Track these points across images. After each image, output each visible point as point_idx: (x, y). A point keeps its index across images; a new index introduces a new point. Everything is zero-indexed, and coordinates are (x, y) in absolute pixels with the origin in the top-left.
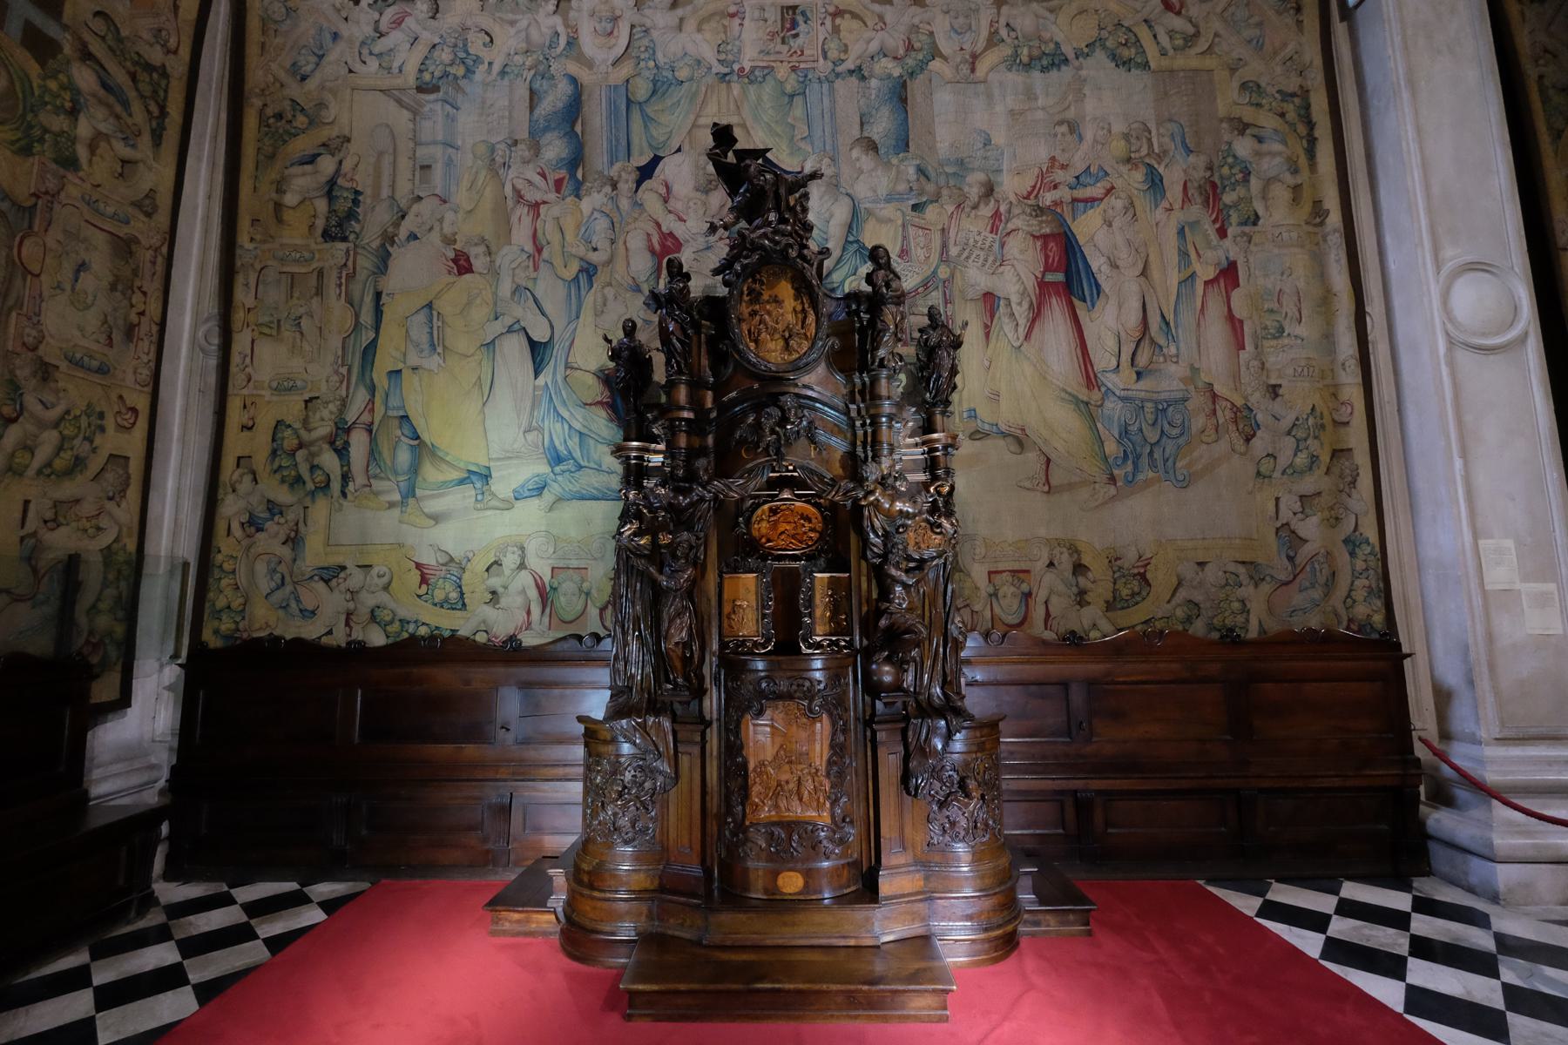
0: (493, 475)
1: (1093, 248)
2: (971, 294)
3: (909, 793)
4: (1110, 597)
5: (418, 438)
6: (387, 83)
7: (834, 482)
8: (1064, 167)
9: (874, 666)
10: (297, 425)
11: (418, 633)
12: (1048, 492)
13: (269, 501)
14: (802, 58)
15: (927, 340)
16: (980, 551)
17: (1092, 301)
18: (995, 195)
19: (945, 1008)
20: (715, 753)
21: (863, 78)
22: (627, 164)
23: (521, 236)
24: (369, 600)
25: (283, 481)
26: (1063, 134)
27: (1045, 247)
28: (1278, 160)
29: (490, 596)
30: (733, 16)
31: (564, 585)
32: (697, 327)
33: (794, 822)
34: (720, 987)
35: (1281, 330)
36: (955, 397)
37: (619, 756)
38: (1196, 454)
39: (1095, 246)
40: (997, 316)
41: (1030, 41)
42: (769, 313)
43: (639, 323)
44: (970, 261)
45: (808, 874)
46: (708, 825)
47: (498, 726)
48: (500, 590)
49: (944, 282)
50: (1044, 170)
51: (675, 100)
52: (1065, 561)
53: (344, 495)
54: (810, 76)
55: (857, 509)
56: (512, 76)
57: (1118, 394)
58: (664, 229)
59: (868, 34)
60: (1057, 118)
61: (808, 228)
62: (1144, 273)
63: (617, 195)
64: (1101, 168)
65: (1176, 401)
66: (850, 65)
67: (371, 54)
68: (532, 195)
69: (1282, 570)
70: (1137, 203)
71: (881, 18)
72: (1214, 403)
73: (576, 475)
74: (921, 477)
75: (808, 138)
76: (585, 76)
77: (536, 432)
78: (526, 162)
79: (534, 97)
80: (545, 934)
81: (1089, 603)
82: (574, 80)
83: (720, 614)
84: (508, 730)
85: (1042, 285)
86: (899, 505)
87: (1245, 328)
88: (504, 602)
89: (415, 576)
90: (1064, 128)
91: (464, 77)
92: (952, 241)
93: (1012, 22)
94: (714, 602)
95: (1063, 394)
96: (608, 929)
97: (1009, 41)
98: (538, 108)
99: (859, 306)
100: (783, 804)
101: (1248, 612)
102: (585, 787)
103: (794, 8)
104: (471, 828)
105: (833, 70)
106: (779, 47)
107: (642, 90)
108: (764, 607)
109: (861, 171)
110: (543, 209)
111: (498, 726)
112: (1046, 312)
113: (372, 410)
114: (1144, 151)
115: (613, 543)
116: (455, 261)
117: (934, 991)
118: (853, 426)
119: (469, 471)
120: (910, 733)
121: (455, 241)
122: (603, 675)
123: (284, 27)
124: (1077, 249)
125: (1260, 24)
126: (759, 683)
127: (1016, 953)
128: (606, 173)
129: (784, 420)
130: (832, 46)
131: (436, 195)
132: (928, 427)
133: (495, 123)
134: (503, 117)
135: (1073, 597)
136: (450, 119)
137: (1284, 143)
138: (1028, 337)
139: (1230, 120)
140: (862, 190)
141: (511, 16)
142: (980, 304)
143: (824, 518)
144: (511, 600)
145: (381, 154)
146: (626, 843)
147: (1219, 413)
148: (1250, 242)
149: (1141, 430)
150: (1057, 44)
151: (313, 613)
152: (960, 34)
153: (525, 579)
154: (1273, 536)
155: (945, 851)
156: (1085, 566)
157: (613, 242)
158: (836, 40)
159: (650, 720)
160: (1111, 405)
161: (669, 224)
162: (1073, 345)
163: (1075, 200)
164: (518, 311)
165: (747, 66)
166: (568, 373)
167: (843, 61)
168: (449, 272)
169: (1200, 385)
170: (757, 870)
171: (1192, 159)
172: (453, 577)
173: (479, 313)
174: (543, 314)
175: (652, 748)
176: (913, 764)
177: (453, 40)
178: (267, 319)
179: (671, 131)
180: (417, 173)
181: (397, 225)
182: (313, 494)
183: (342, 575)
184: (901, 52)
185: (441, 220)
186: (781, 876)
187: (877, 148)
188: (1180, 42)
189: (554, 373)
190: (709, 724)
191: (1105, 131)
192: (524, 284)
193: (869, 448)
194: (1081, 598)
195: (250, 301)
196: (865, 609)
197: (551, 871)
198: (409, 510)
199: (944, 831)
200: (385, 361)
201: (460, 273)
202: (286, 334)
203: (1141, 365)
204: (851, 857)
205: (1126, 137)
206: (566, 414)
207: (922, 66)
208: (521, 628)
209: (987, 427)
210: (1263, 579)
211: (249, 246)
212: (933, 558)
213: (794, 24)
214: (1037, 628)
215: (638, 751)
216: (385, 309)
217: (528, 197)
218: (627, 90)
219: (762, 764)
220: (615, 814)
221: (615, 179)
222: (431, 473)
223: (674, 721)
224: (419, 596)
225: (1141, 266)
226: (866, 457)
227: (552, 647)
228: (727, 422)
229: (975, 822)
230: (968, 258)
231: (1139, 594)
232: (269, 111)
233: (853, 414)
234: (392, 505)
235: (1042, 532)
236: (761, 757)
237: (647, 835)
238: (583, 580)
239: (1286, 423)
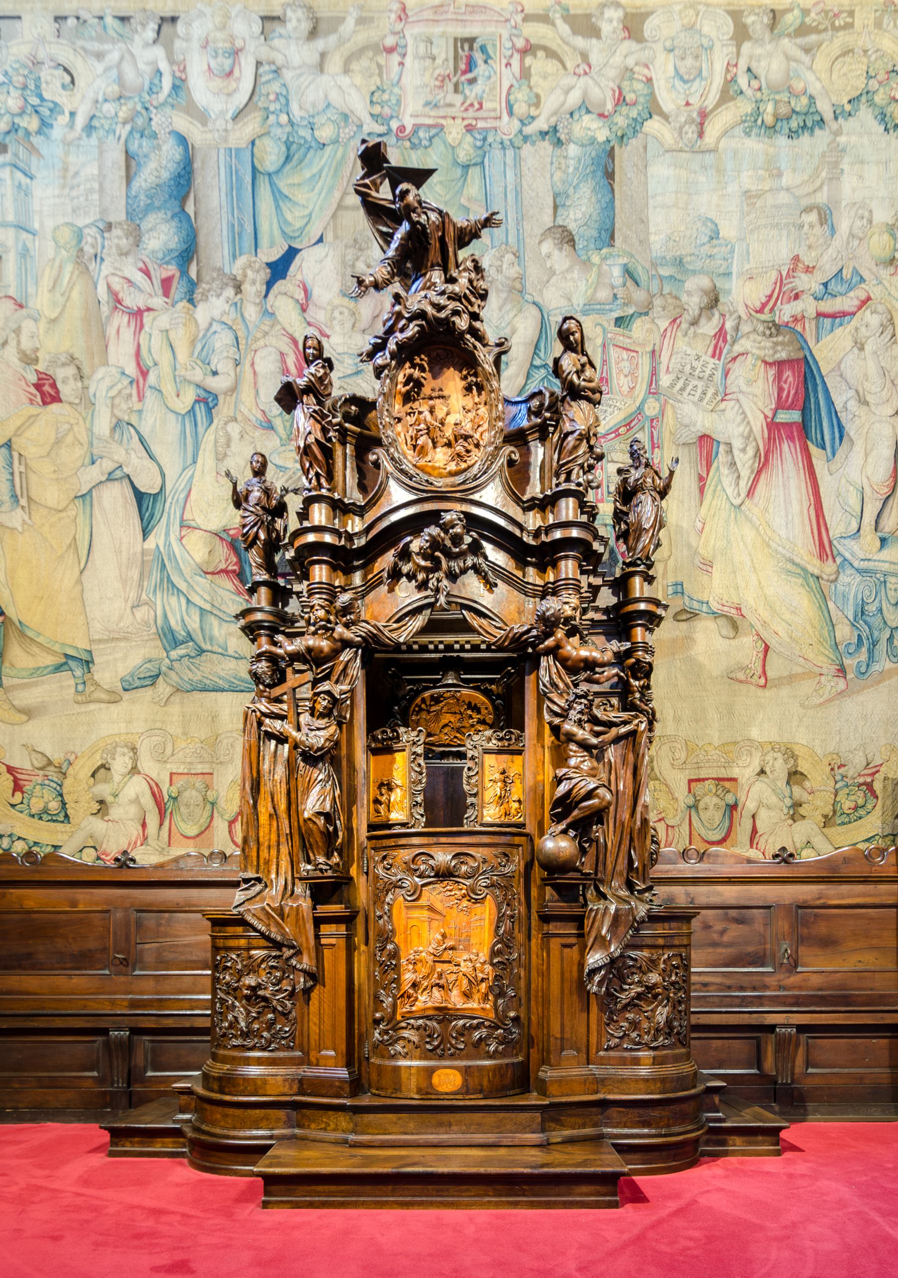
0: (96, 660)
1: (839, 379)
4: (828, 810)
8: (809, 270)
12: (765, 686)
14: (480, 114)
17: (833, 447)
18: (720, 306)
21: (559, 143)
22: (253, 259)
26: (811, 226)
27: (779, 376)
29: (97, 806)
30: (390, 50)
31: (187, 794)
39: (841, 376)
40: (715, 465)
41: (779, 92)
44: (685, 394)
48: (109, 799)
49: (652, 420)
50: (784, 274)
51: (315, 170)
52: (779, 768)
54: (490, 139)
56: (102, 133)
57: (856, 564)
60: (805, 202)
63: (242, 300)
64: (856, 272)
66: (542, 124)
68: (133, 300)
71: (585, 57)
73: (197, 661)
76: (197, 135)
77: (146, 607)
78: (123, 254)
82: (182, 140)
85: (773, 426)
88: (115, 813)
91: (39, 132)
92: (663, 368)
93: (754, 66)
95: (789, 566)
97: (749, 92)
98: (137, 179)
103: (471, 41)
105: (521, 131)
106: (452, 98)
109: (552, 272)
110: (147, 318)
112: (775, 460)
116: (38, 387)
119: (66, 655)
121: (36, 360)
124: (818, 381)
128: (227, 270)
130: (520, 96)
131: (10, 297)
133: (82, 199)
134: (91, 191)
135: (786, 811)
136: (23, 192)
138: (750, 493)
141: (95, 46)
142: (695, 450)
143: (496, 708)
149: (880, 610)
150: (811, 97)
152: (685, 82)
153: (137, 787)
156: (802, 774)
157: (237, 363)
158: (525, 88)
163: (820, 315)
165: (409, 123)
166: (183, 533)
167: (533, 118)
172: (52, 784)
173: (72, 455)
174: (151, 457)
177: (21, 79)
179: (310, 215)
184: (609, 106)
185: (18, 331)
187: (573, 240)
189: (167, 534)
191: (865, 220)
192: (126, 418)
194: (795, 811)
201: (45, 403)
203: (887, 529)
207: (636, 126)
208: (135, 843)
209: (696, 605)
213: (470, 65)
217: (127, 302)
218: (253, 155)
221: (239, 278)
224: (13, 806)
230: (683, 389)
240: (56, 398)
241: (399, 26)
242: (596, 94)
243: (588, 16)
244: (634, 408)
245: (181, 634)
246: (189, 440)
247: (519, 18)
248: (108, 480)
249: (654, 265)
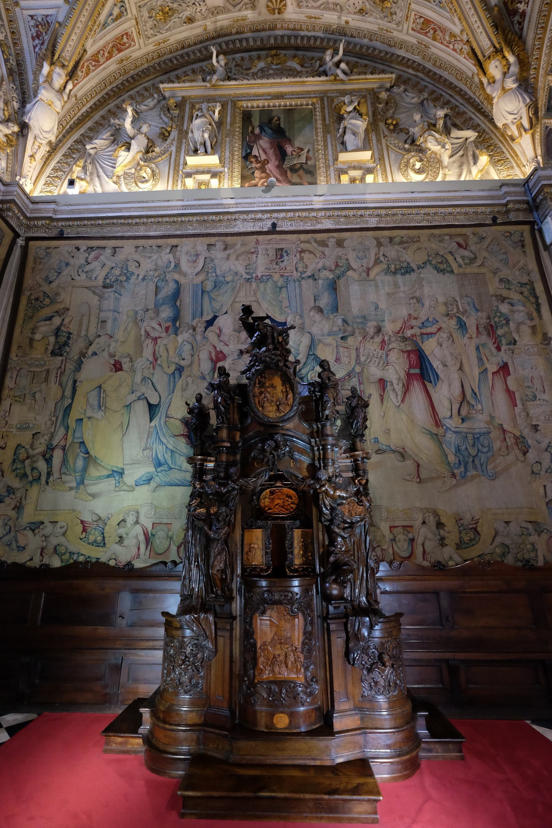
2: (373, 379)
3: (349, 663)
4: (458, 541)
5: (88, 453)
6: (89, 284)
7: (303, 479)
8: (416, 318)
9: (327, 585)
10: (28, 447)
11: (79, 560)
12: (420, 482)
13: (8, 486)
15: (350, 404)
16: (384, 514)
17: (435, 382)
19: (376, 813)
20: (238, 636)
21: (315, 279)
23: (148, 353)
24: (54, 541)
25: (17, 476)
26: (414, 303)
27: (408, 356)
28: (522, 314)
29: (118, 539)
31: (159, 533)
32: (232, 399)
33: (283, 681)
34: (238, 794)
35: (535, 397)
36: (367, 432)
37: (184, 637)
38: (497, 462)
42: (269, 393)
43: (204, 395)
45: (292, 715)
46: (234, 682)
47: (118, 615)
48: (124, 536)
52: (432, 520)
53: (47, 483)
55: (316, 494)
58: (218, 349)
59: (317, 260)
60: (411, 296)
61: (289, 352)
62: (461, 369)
64: (434, 319)
65: (484, 434)
67: (83, 271)
68: (154, 334)
70: (454, 335)
71: (323, 253)
72: (504, 434)
73: (168, 473)
74: (350, 475)
75: (289, 307)
76: (182, 280)
77: (148, 450)
78: (152, 319)
79: (157, 289)
80: (136, 752)
81: (447, 545)
82: (177, 282)
83: (242, 552)
84: (123, 618)
85: (409, 375)
86: (338, 493)
87: (517, 396)
88: (126, 542)
89: (80, 528)
90: (414, 301)
92: (361, 354)
93: (385, 254)
94: (239, 546)
95: (423, 430)
96: (173, 750)
97: (385, 262)
99: (315, 388)
100: (277, 669)
101: (536, 550)
102: (164, 655)
103: (282, 249)
104: (99, 679)
106: (275, 266)
107: (209, 286)
108: (266, 548)
109: (315, 322)
110: (159, 341)
111: (118, 616)
112: (411, 388)
113: (66, 439)
114: (455, 310)
115: (187, 510)
116: (114, 365)
117: (369, 800)
118: (313, 450)
119: (113, 471)
120: (349, 625)
122: (177, 585)
123: (44, 261)
125: (505, 253)
126: (263, 595)
127: (418, 772)
129: (277, 447)
130: (300, 265)
132: (352, 449)
137: (524, 305)
139: (496, 296)
140: (315, 330)
141: (149, 255)
142: (378, 385)
143: (299, 496)
144: (130, 542)
145: (83, 316)
146: (186, 693)
147: (508, 440)
148: (513, 353)
149: (467, 449)
151: (24, 548)
153: (138, 529)
154: (545, 506)
155: (372, 700)
156: (443, 524)
157: (192, 356)
158: (302, 263)
159: (202, 616)
160: (450, 436)
161: (220, 347)
162: (427, 405)
163: (422, 334)
164: (143, 389)
168: (111, 371)
169: (496, 425)
170: (261, 712)
171: (479, 314)
173: (124, 390)
174: (156, 390)
175: (202, 632)
176: (351, 645)
178: (19, 394)
180: (99, 325)
181: (87, 348)
182: (31, 482)
183: (41, 527)
184: (333, 267)
185: (109, 346)
186: (276, 716)
188: (467, 261)
189: (160, 420)
190: (235, 618)
193: (321, 462)
194: (442, 542)
195: (12, 385)
196: (321, 550)
197: (142, 710)
198: (80, 491)
199: (371, 688)
200: (74, 415)
201: (116, 371)
202: (28, 401)
204: (317, 703)
205: (446, 304)
206: (164, 441)
207: (343, 273)
209: (384, 447)
210: (543, 531)
211: (15, 358)
212: (358, 522)
213: (282, 256)
214: (419, 559)
215: (194, 635)
216: (77, 388)
219: (265, 644)
220: (180, 674)
222: (93, 472)
223: (215, 617)
224: (81, 539)
225: (459, 366)
226: (320, 466)
227: (150, 569)
228: (247, 449)
229: (389, 682)
230: (370, 362)
231: (474, 539)
232: (33, 297)
233: (313, 444)
234: (71, 489)
235: (418, 504)
236: (265, 640)
237: (198, 687)
238: (169, 530)
239: (544, 445)
240: (121, 369)
241: (256, 246)
242: (328, 264)
243: (324, 241)
244: (351, 369)
245: (162, 460)
246: (172, 384)
247: (299, 242)
248: (138, 399)
249: (354, 318)
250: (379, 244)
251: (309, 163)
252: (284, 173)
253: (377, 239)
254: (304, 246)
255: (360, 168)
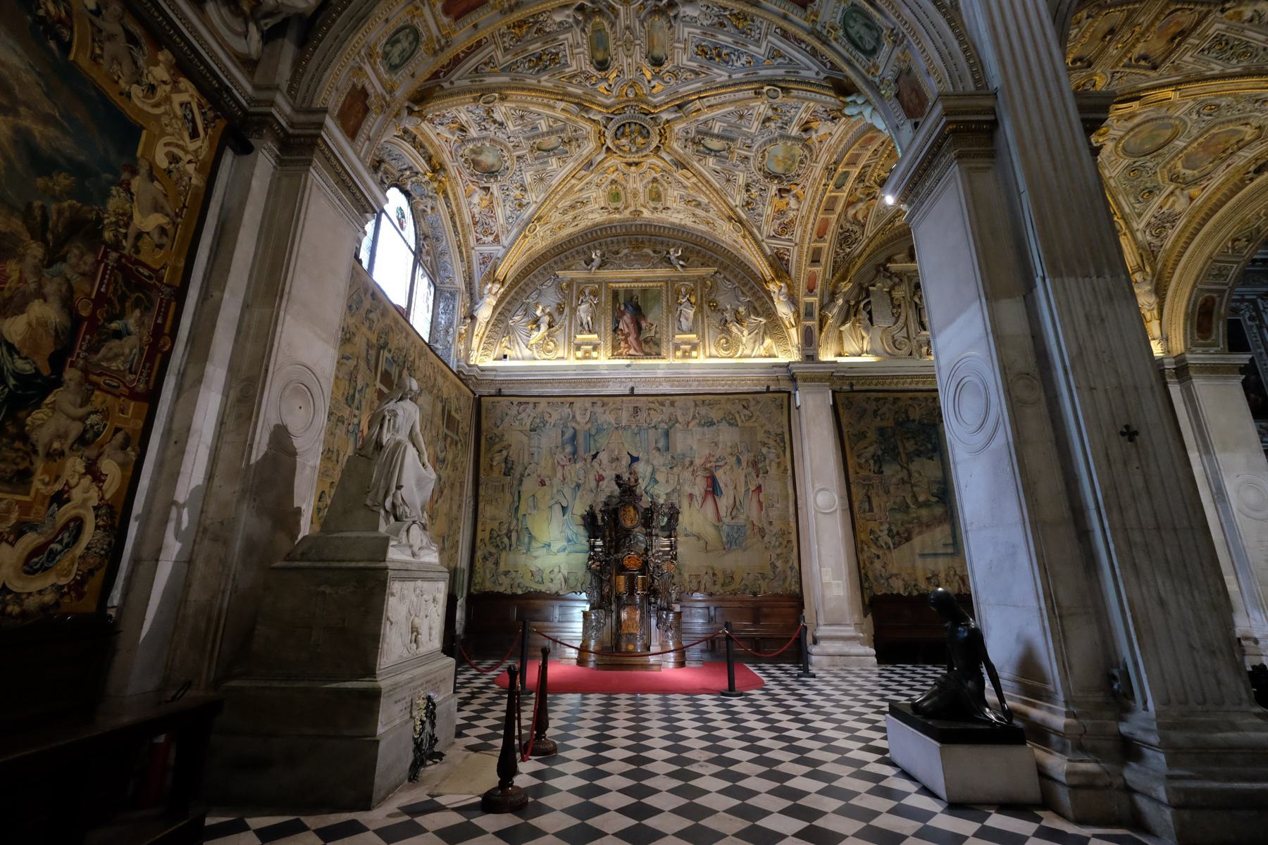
23: (559, 475)
52: (710, 572)
68: (562, 463)
69: (771, 575)
76: (577, 427)
107: (593, 432)
140: (655, 462)
153: (560, 575)
161: (601, 472)
173: (548, 498)
200: (521, 512)
222: (534, 544)
250: (696, 405)
251: (657, 336)
252: (639, 344)
253: (695, 401)
254: (652, 405)
255: (689, 344)
